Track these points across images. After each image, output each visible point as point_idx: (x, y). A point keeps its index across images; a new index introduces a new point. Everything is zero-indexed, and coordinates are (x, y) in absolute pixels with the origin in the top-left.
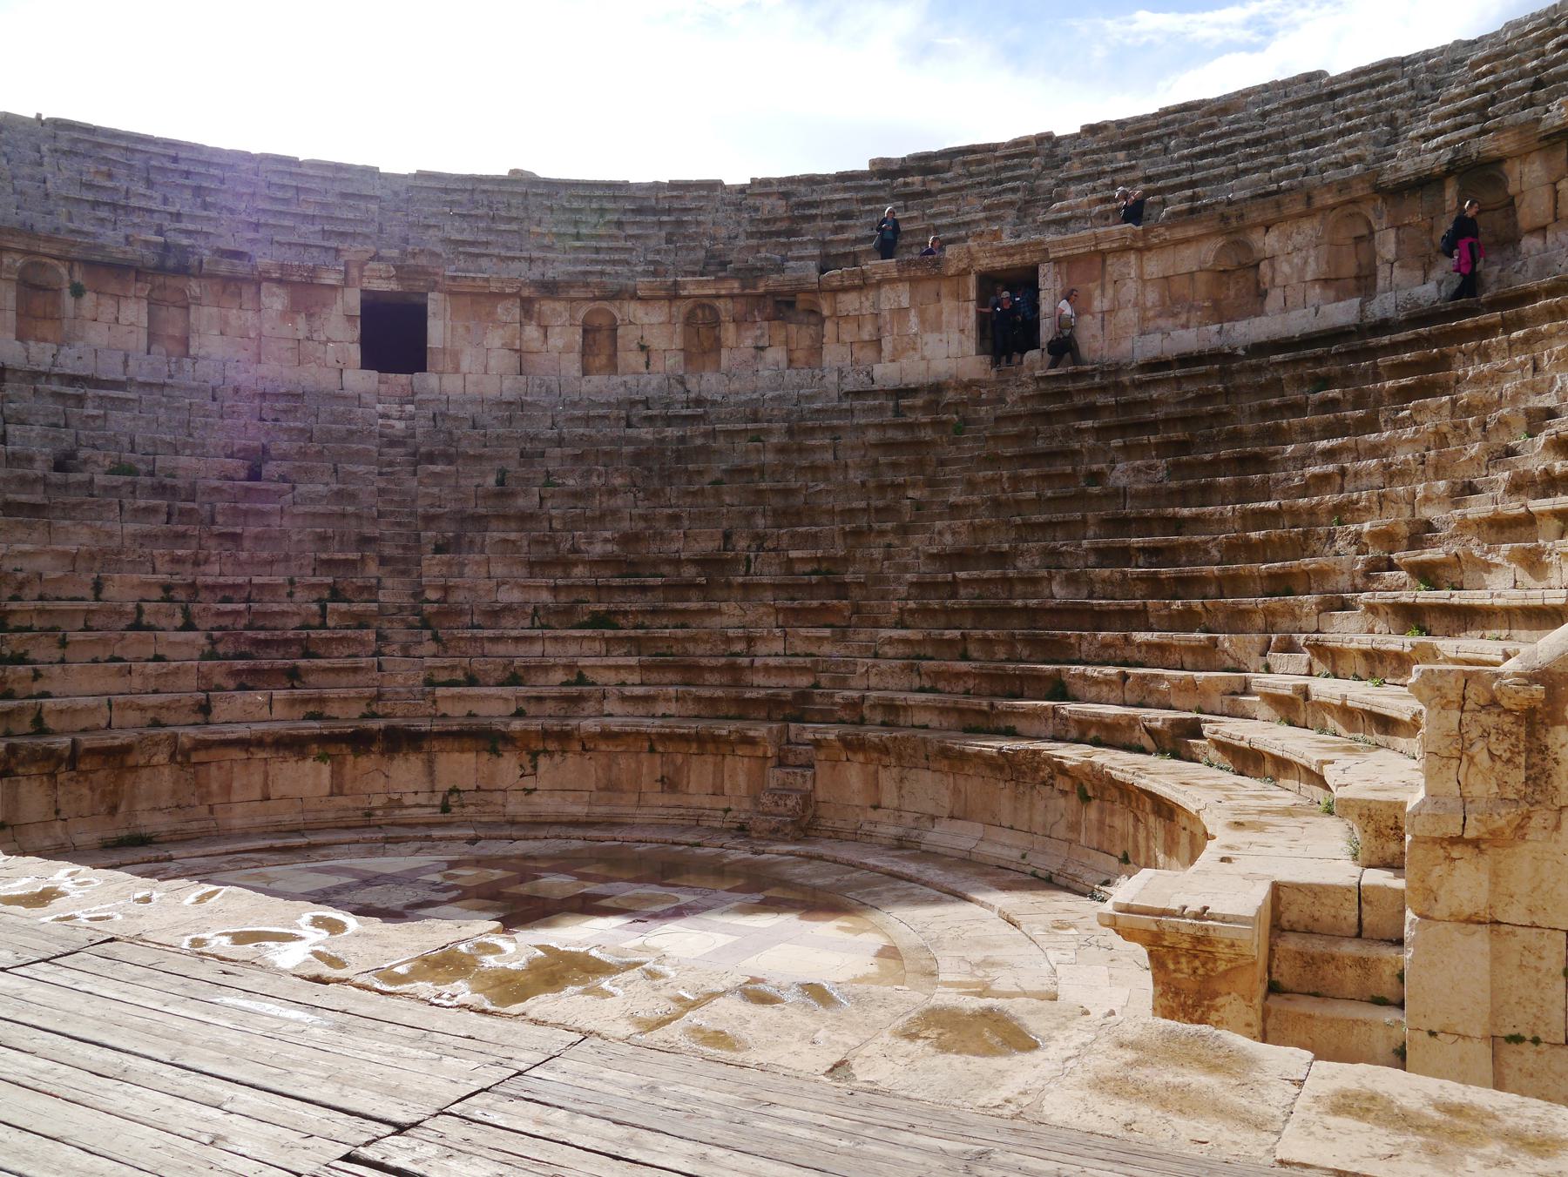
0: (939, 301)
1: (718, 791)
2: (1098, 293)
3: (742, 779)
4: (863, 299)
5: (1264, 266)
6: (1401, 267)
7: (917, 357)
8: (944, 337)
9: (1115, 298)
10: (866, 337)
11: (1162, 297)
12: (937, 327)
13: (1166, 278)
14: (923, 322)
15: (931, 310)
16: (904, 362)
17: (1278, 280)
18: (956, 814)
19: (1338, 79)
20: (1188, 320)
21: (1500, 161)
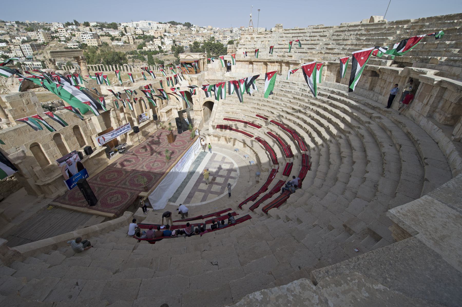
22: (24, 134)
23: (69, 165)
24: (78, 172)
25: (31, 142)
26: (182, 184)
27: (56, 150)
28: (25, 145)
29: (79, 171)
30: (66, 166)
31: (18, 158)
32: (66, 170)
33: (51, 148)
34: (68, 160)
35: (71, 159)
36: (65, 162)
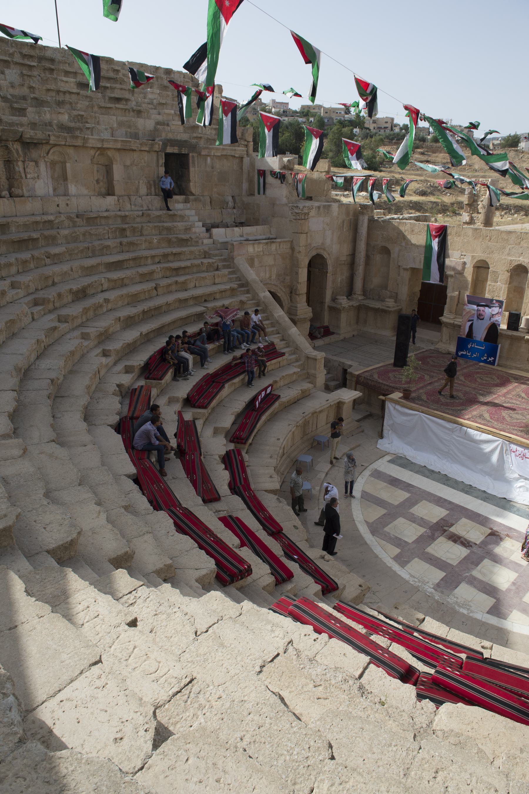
22: (481, 240)
23: (478, 318)
24: (483, 341)
25: (480, 255)
26: (456, 482)
27: (502, 291)
28: (473, 256)
29: (486, 339)
30: (474, 314)
31: (454, 269)
32: (469, 321)
33: (499, 283)
34: (481, 308)
35: (487, 309)
36: (475, 307)
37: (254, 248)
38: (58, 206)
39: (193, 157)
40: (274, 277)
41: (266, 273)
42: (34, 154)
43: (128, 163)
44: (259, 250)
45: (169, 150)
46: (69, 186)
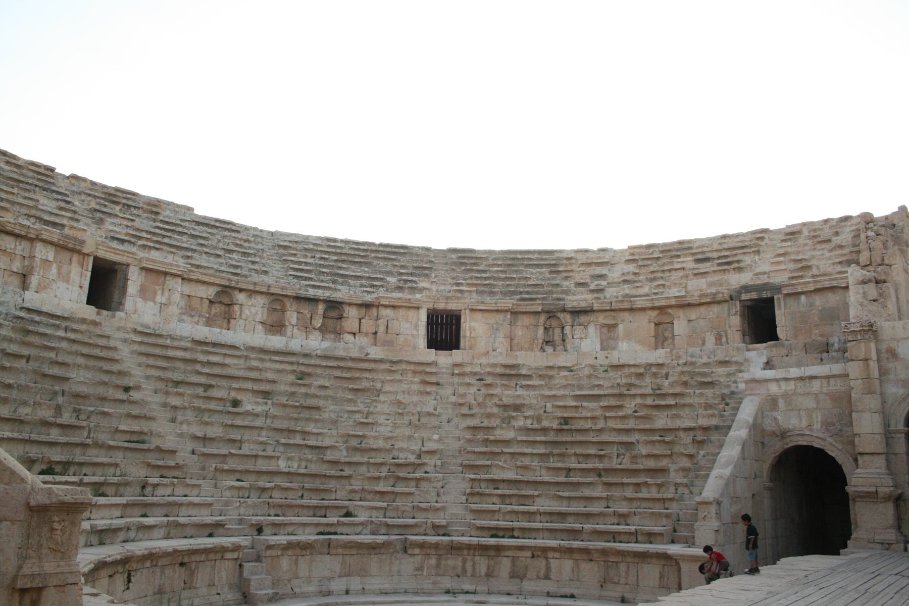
0: (70, 264)
1: (211, 585)
2: (159, 292)
3: (224, 574)
4: (18, 244)
5: (236, 308)
6: (299, 329)
7: (52, 295)
8: (70, 287)
9: (169, 299)
10: (15, 270)
11: (186, 305)
12: (67, 280)
13: (189, 296)
14: (59, 273)
15: (65, 268)
16: (43, 294)
17: (243, 316)
18: (343, 574)
19: (196, 215)
20: (198, 321)
21: (342, 303)
37: (780, 387)
38: (596, 358)
39: (779, 299)
40: (817, 426)
41: (801, 420)
42: (583, 319)
43: (693, 317)
44: (789, 388)
45: (744, 297)
46: (620, 343)
